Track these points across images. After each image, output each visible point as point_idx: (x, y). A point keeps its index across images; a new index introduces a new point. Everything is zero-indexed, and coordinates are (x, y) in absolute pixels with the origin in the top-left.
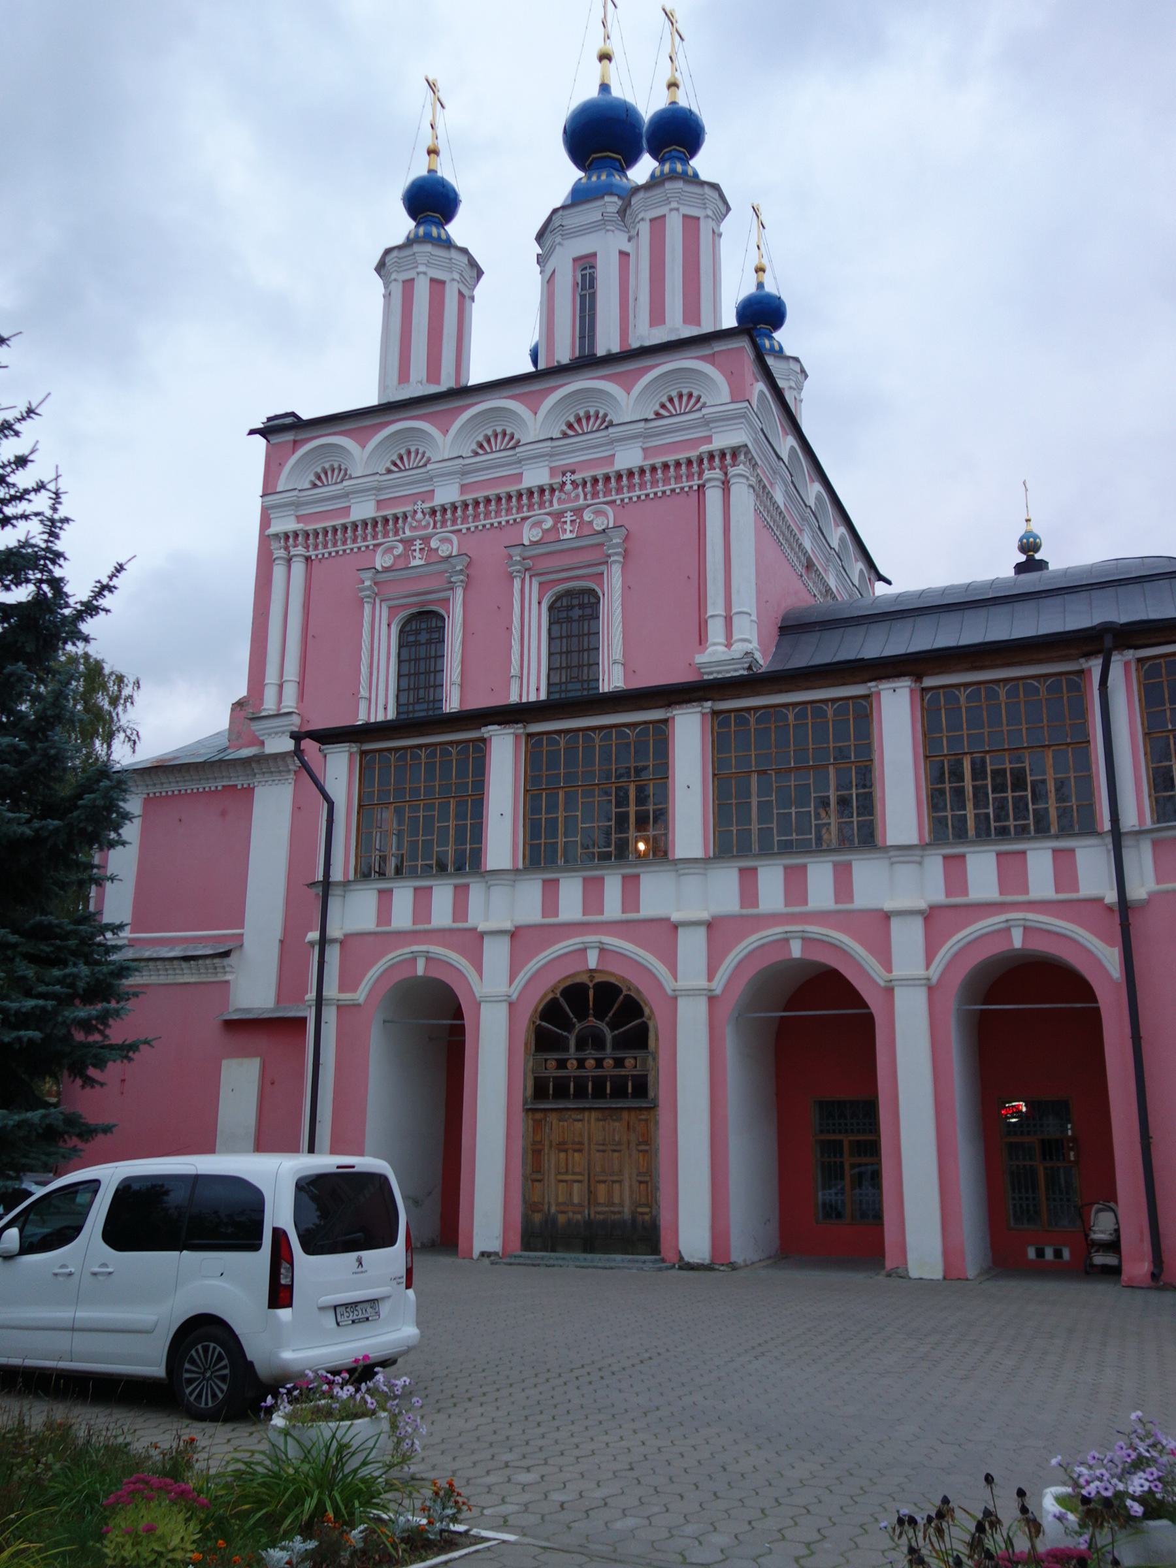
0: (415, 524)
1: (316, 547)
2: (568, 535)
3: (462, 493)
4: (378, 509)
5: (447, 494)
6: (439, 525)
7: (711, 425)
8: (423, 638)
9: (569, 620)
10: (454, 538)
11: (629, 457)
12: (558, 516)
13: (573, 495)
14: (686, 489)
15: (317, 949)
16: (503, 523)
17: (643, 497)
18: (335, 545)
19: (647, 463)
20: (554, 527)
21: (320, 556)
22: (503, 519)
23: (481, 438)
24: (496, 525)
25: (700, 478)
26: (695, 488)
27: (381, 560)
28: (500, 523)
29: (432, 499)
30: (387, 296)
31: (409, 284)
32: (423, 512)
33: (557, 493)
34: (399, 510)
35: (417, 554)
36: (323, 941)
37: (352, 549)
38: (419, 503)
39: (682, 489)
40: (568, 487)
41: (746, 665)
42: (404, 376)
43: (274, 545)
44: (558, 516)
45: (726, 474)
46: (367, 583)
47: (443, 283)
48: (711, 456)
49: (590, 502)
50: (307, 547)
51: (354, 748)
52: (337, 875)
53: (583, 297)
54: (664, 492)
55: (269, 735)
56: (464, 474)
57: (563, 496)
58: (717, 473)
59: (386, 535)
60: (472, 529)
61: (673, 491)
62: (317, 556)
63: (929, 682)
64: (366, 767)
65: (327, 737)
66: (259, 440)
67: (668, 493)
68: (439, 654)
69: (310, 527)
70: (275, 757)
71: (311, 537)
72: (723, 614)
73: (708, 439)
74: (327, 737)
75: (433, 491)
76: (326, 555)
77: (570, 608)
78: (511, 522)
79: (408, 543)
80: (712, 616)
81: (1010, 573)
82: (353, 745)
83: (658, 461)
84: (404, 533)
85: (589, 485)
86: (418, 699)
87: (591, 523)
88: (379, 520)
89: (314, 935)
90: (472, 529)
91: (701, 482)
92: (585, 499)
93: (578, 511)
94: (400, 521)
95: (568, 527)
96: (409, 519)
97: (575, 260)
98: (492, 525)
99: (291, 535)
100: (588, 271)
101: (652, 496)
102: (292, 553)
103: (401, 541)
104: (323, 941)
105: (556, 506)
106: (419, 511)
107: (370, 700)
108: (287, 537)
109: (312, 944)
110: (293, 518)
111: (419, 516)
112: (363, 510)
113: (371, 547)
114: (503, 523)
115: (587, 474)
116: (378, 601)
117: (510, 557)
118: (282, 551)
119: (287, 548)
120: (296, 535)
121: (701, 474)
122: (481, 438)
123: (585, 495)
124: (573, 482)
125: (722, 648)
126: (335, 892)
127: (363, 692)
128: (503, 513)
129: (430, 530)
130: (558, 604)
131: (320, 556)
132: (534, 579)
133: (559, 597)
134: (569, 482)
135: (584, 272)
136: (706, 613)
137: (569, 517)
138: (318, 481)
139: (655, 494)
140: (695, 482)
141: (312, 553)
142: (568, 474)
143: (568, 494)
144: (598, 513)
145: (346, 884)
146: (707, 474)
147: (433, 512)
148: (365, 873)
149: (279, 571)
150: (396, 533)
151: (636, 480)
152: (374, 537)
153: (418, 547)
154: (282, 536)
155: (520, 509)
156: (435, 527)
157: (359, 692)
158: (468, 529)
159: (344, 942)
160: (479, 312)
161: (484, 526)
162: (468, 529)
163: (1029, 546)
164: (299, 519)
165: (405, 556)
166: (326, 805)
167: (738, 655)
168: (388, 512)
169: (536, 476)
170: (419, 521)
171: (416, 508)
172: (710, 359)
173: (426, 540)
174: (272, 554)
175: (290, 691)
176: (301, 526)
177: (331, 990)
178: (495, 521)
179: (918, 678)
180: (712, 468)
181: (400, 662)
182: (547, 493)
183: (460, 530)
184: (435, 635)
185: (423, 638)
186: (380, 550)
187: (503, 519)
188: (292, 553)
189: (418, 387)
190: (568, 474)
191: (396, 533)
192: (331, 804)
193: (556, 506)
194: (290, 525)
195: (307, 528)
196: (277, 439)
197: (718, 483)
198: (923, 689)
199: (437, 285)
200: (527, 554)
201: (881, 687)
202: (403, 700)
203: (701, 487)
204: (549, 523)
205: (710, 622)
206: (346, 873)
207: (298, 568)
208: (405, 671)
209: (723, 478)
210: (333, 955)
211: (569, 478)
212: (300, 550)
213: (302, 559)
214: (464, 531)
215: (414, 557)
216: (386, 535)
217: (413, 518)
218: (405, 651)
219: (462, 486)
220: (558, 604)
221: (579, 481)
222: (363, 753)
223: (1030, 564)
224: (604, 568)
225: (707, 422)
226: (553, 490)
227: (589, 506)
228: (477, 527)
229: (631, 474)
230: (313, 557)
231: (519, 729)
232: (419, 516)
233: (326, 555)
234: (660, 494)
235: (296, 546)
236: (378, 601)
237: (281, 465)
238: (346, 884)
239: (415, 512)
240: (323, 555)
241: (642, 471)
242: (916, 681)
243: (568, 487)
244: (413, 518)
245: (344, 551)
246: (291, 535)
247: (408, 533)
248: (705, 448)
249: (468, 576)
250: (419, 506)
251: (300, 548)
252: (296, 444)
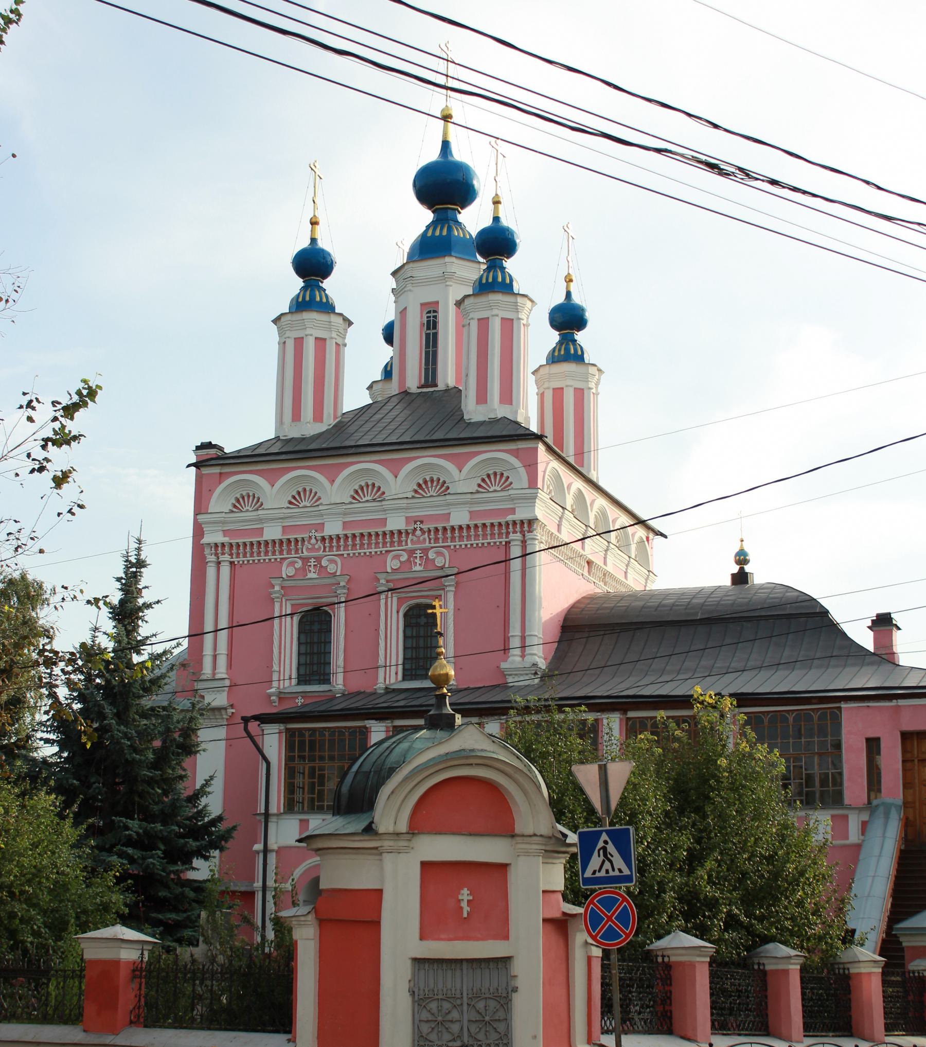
0: (310, 546)
1: (238, 555)
2: (418, 568)
3: (344, 529)
4: (284, 533)
5: (333, 528)
6: (327, 549)
7: (515, 502)
8: (316, 627)
9: (418, 625)
10: (338, 560)
11: (460, 517)
12: (411, 552)
13: (421, 538)
14: (498, 544)
15: (261, 856)
16: (373, 553)
17: (469, 546)
18: (252, 555)
19: (472, 523)
20: (408, 559)
21: (241, 562)
22: (373, 551)
23: (357, 487)
24: (368, 554)
25: (507, 537)
26: (504, 543)
27: (287, 571)
28: (371, 553)
29: (323, 530)
30: (282, 345)
31: (299, 342)
32: (315, 538)
33: (410, 536)
34: (299, 536)
35: (312, 569)
36: (266, 851)
37: (264, 560)
38: (313, 531)
39: (495, 543)
40: (418, 533)
41: (533, 672)
42: (297, 416)
43: (207, 551)
44: (411, 552)
45: (524, 536)
46: (277, 588)
47: (325, 340)
48: (514, 523)
49: (433, 545)
50: (231, 555)
51: (282, 727)
52: (273, 809)
53: (428, 335)
54: (483, 544)
55: (208, 692)
56: (345, 514)
57: (415, 538)
58: (518, 536)
59: (289, 552)
60: (351, 555)
61: (489, 543)
62: (239, 562)
63: (631, 714)
64: (293, 743)
65: (264, 719)
66: (193, 469)
67: (486, 545)
68: (327, 640)
69: (234, 541)
70: (214, 710)
71: (234, 548)
72: (520, 634)
73: (512, 511)
74: (264, 719)
75: (323, 524)
76: (246, 562)
77: (419, 616)
78: (379, 553)
79: (305, 560)
80: (512, 636)
81: (727, 582)
82: (281, 725)
83: (479, 522)
84: (303, 553)
85: (432, 533)
86: (313, 672)
87: (433, 560)
88: (284, 541)
89: (259, 847)
90: (351, 555)
91: (507, 540)
92: (430, 543)
93: (425, 551)
94: (300, 543)
95: (418, 561)
96: (306, 543)
97: (422, 305)
98: (365, 553)
99: (219, 545)
100: (432, 314)
101: (475, 545)
102: (220, 559)
103: (300, 558)
104: (266, 851)
105: (410, 545)
106: (313, 537)
107: (280, 672)
108: (216, 545)
109: (258, 852)
110: (221, 533)
111: (313, 541)
112: (273, 533)
113: (278, 560)
114: (373, 553)
115: (432, 526)
116: (284, 600)
117: (378, 580)
118: (213, 556)
119: (216, 554)
120: (223, 545)
121: (508, 533)
122: (357, 487)
123: (430, 539)
124: (421, 529)
125: (519, 659)
126: (273, 820)
127: (276, 668)
128: (373, 546)
129: (321, 553)
130: (410, 613)
131: (241, 562)
132: (394, 595)
133: (411, 609)
134: (418, 529)
135: (429, 315)
136: (509, 633)
137: (418, 554)
138: (237, 506)
139: (477, 544)
140: (504, 540)
141: (235, 560)
142: (418, 523)
143: (419, 537)
144: (439, 554)
145: (279, 815)
146: (512, 536)
147: (323, 539)
148: (290, 807)
149: (211, 571)
150: (297, 552)
151: (465, 533)
152: (281, 552)
153: (312, 564)
154: (213, 545)
155: (384, 544)
156: (324, 551)
157: (272, 666)
158: (348, 554)
159: (278, 852)
160: (349, 354)
161: (359, 553)
162: (348, 554)
163: (742, 559)
164: (226, 533)
165: (304, 569)
166: (265, 765)
167: (528, 665)
168: (292, 537)
169: (396, 523)
170: (313, 545)
171: (311, 534)
172: (516, 453)
173: (318, 559)
174: (205, 558)
175: (222, 661)
176: (226, 540)
177: (270, 883)
178: (367, 551)
179: (625, 711)
180: (515, 532)
181: (300, 644)
182: (404, 535)
183: (343, 555)
184: (325, 627)
185: (316, 627)
186: (286, 563)
187: (373, 551)
188: (220, 559)
189: (309, 428)
190: (418, 523)
191: (297, 552)
192: (268, 764)
193: (410, 545)
194: (219, 538)
195: (231, 541)
196: (205, 471)
197: (519, 543)
198: (628, 718)
199: (321, 342)
200: (389, 578)
201: (603, 716)
202: (302, 672)
203: (508, 543)
204: (404, 557)
205: (511, 639)
206: (279, 808)
207: (225, 570)
208: (303, 651)
209: (522, 539)
210: (272, 859)
211: (418, 525)
212: (227, 557)
213: (227, 564)
214: (345, 556)
215: (310, 571)
216: (289, 552)
217: (309, 542)
218: (302, 636)
219: (344, 523)
220: (410, 613)
221: (426, 530)
222: (287, 730)
223: (740, 578)
224: (442, 592)
225: (512, 499)
226: (407, 533)
227: (432, 547)
228: (354, 554)
229: (461, 528)
230: (236, 563)
231: (388, 723)
232: (313, 541)
233: (246, 562)
234: (480, 545)
235: (223, 554)
236: (284, 600)
237: (211, 491)
238: (279, 815)
239: (310, 537)
240: (243, 562)
241: (468, 527)
242: (623, 714)
243: (418, 533)
244: (309, 542)
245: (259, 560)
246: (219, 545)
247: (305, 553)
248: (510, 518)
249: (348, 589)
250: (313, 533)
251: (226, 555)
252: (222, 477)
